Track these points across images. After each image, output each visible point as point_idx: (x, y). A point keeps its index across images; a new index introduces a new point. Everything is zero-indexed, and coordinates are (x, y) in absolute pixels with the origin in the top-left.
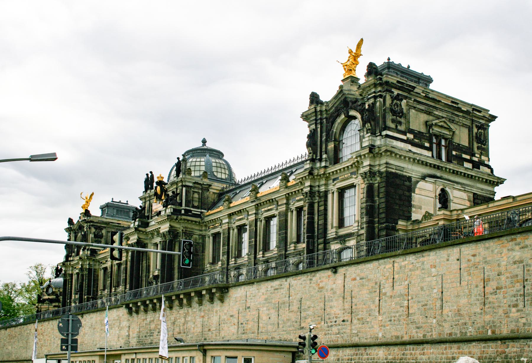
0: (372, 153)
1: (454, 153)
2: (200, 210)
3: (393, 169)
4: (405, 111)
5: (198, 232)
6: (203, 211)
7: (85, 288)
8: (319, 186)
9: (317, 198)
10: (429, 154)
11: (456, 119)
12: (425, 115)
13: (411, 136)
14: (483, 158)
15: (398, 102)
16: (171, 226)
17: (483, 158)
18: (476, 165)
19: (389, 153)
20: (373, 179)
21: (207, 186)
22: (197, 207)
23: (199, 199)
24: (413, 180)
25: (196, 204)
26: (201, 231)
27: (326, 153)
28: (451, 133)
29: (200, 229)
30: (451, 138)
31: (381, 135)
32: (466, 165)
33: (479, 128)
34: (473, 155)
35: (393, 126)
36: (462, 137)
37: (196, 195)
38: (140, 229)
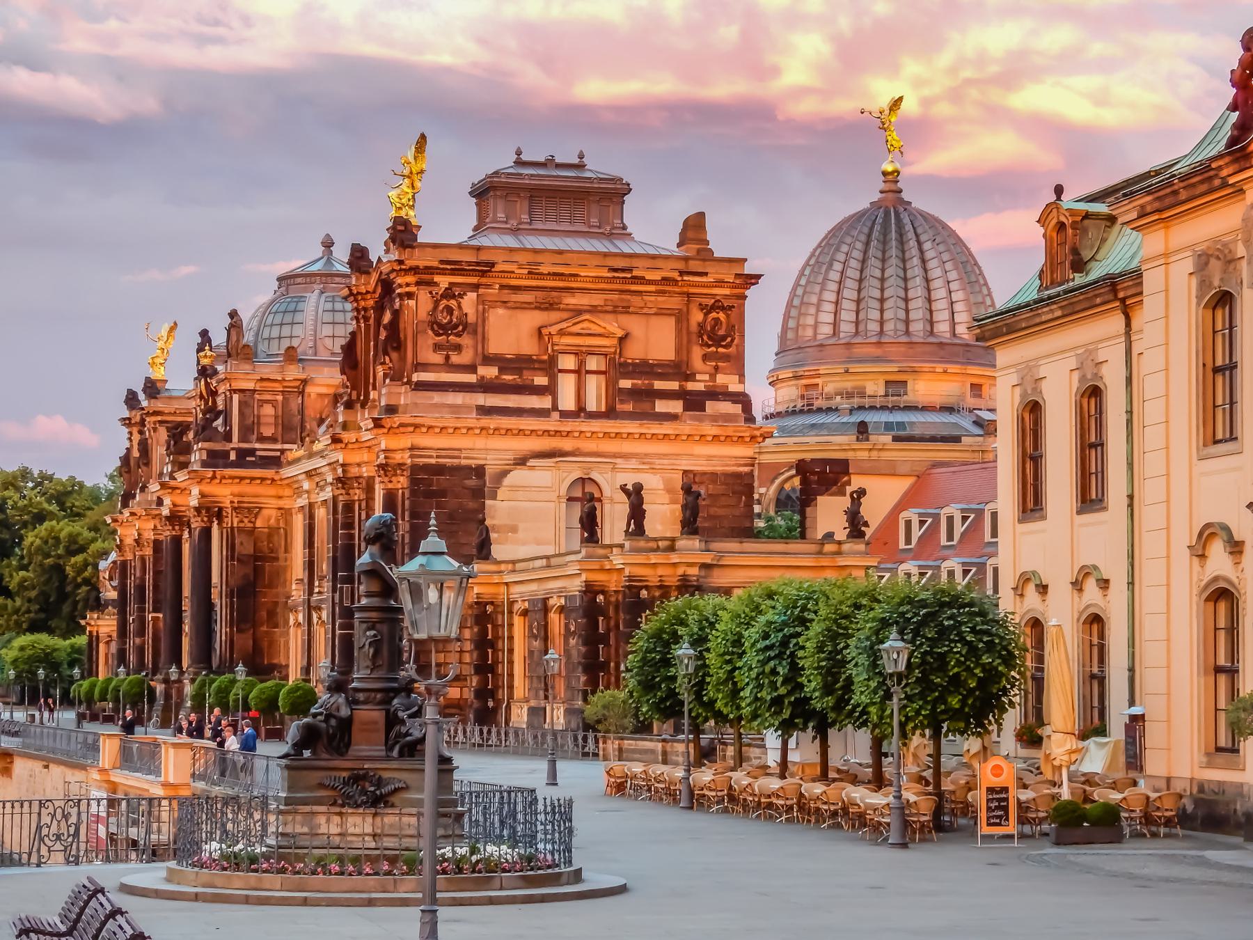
0: (383, 427)
1: (626, 384)
2: (279, 446)
3: (431, 457)
4: (471, 319)
5: (275, 503)
6: (286, 446)
7: (149, 594)
8: (359, 465)
9: (357, 491)
10: (545, 402)
11: (636, 300)
12: (537, 313)
13: (490, 372)
14: (721, 379)
15: (453, 303)
16: (203, 495)
17: (721, 379)
18: (695, 402)
19: (411, 429)
20: (394, 479)
21: (297, 383)
22: (273, 439)
23: (276, 417)
24: (489, 471)
25: (268, 431)
26: (280, 497)
27: (374, 388)
28: (615, 342)
29: (281, 493)
30: (615, 353)
31: (409, 382)
32: (661, 406)
33: (707, 310)
34: (690, 377)
35: (438, 358)
36: (656, 340)
37: (268, 410)
38: (173, 483)
